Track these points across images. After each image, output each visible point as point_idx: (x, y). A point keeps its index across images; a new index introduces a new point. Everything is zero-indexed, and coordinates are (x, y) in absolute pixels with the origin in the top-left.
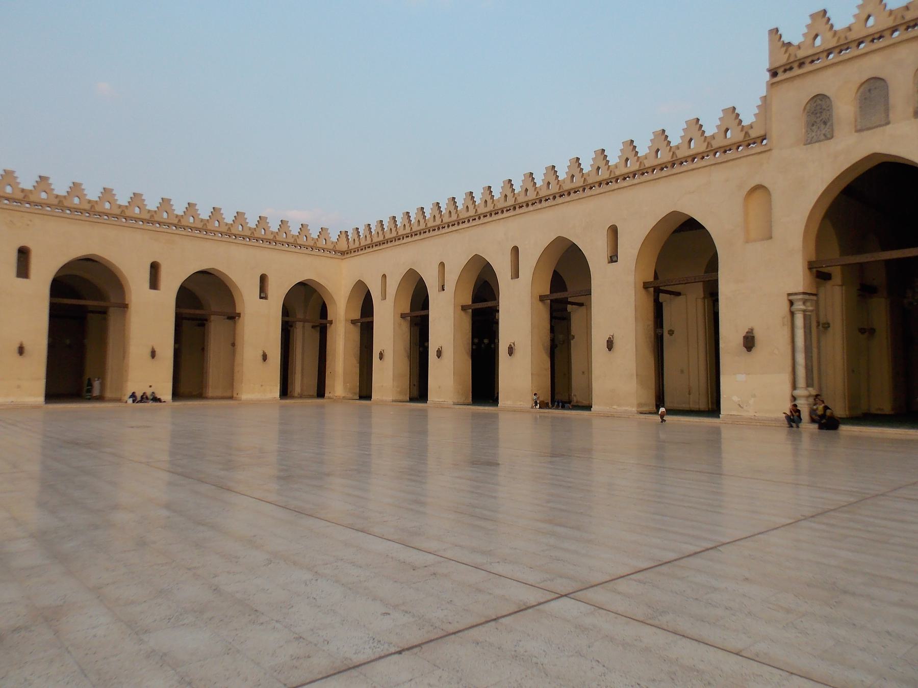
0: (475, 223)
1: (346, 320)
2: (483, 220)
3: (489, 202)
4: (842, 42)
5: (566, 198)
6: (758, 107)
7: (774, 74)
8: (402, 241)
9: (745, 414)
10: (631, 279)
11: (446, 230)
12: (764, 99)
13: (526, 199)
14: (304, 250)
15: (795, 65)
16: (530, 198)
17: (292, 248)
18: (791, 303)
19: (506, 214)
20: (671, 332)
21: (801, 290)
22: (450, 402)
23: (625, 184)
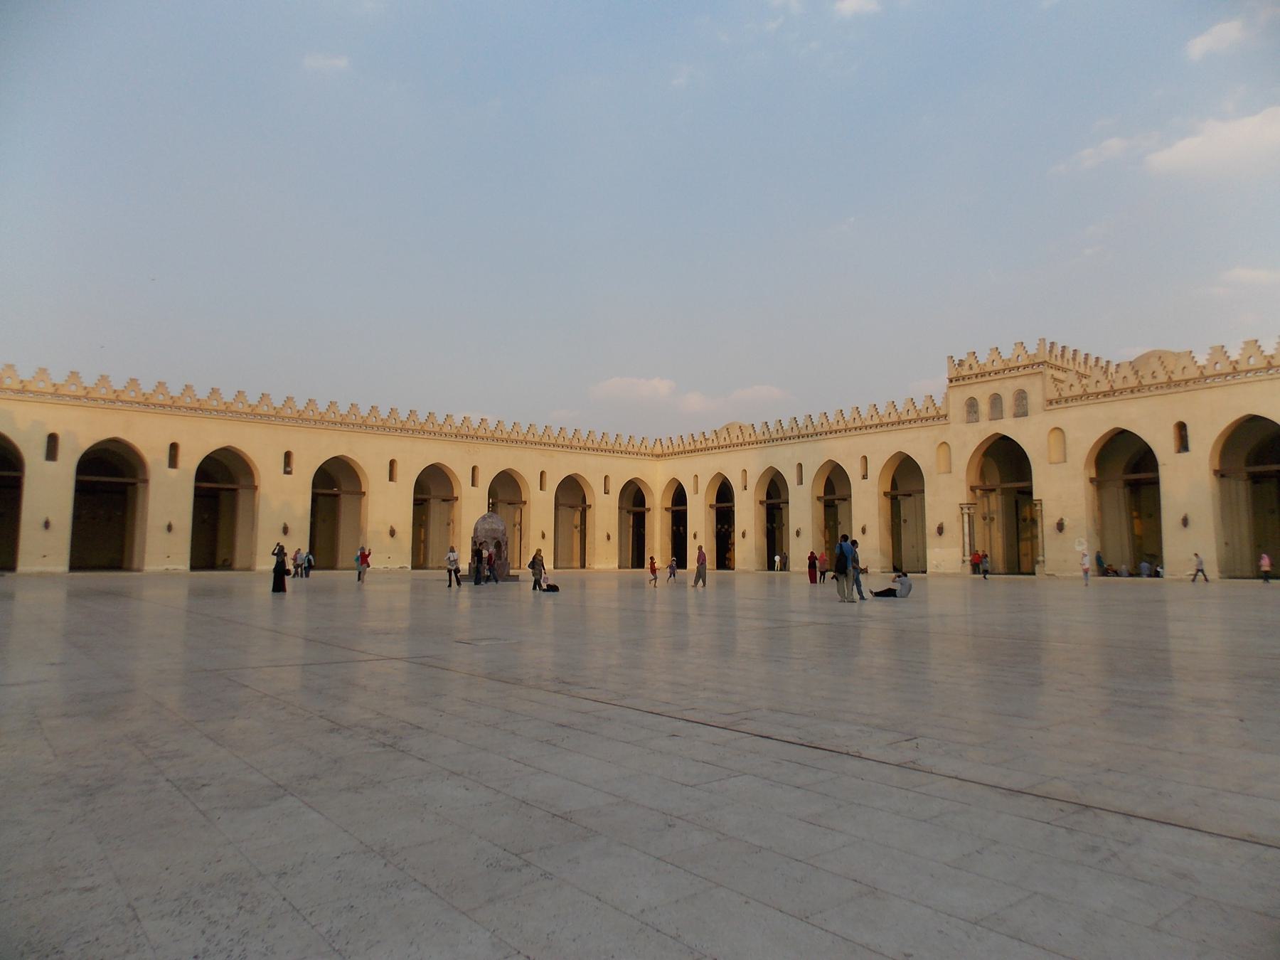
0: (769, 444)
1: (662, 508)
2: (775, 443)
5: (834, 435)
7: (951, 381)
9: (939, 571)
10: (876, 490)
11: (747, 447)
12: (946, 394)
14: (631, 456)
15: (961, 378)
16: (809, 432)
17: (624, 455)
18: (962, 508)
19: (792, 441)
21: (966, 502)
22: (754, 570)
23: (871, 431)
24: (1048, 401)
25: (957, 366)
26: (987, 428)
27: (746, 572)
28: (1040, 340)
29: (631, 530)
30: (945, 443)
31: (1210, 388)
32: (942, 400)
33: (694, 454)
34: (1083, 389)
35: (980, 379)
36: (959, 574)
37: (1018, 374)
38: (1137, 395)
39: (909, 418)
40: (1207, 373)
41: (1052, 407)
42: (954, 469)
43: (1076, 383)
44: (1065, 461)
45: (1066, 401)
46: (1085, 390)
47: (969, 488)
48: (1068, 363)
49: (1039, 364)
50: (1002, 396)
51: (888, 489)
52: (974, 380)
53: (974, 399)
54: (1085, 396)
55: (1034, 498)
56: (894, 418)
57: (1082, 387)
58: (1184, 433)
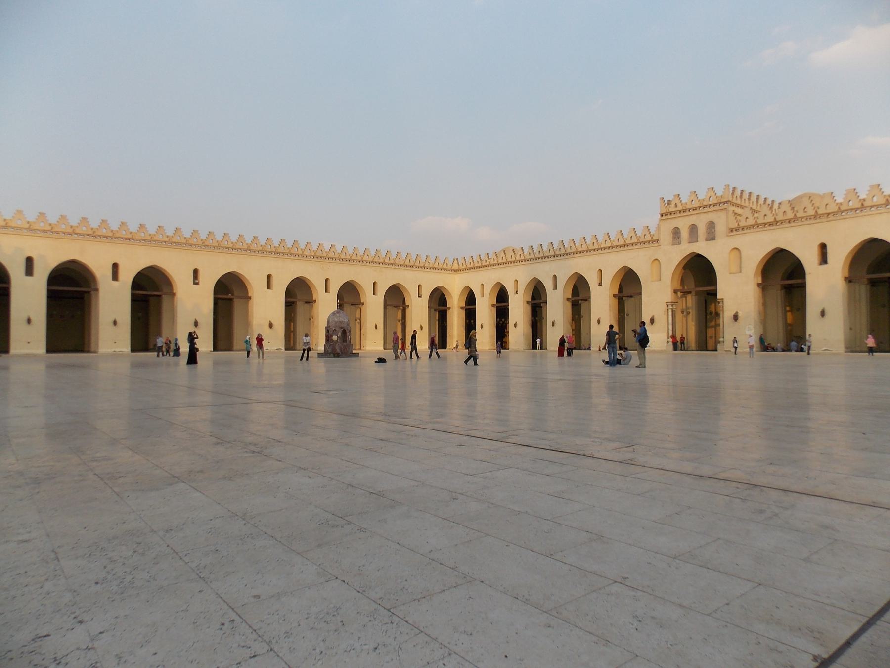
0: (534, 262)
1: (458, 307)
3: (541, 252)
4: (684, 208)
5: (579, 255)
6: (656, 228)
7: (662, 216)
8: (492, 267)
10: (608, 293)
11: (518, 263)
13: (560, 253)
14: (437, 270)
15: (669, 214)
17: (432, 270)
18: (668, 306)
19: (550, 259)
20: (628, 315)
21: (670, 301)
22: (522, 349)
23: (605, 251)
24: (729, 229)
25: (666, 205)
26: (686, 249)
27: (516, 351)
28: (725, 185)
29: (437, 322)
30: (656, 259)
31: (844, 219)
32: (655, 229)
33: (480, 269)
34: (754, 221)
35: (682, 214)
36: (665, 351)
37: (710, 210)
38: (793, 224)
39: (632, 242)
40: (843, 208)
41: (732, 234)
42: (662, 278)
43: (750, 215)
44: (741, 272)
45: (743, 229)
46: (756, 221)
47: (673, 291)
48: (745, 202)
49: (724, 203)
50: (698, 226)
51: (617, 293)
52: (679, 215)
53: (678, 228)
54: (757, 225)
55: (718, 298)
56: (621, 242)
57: (754, 219)
58: (824, 251)
